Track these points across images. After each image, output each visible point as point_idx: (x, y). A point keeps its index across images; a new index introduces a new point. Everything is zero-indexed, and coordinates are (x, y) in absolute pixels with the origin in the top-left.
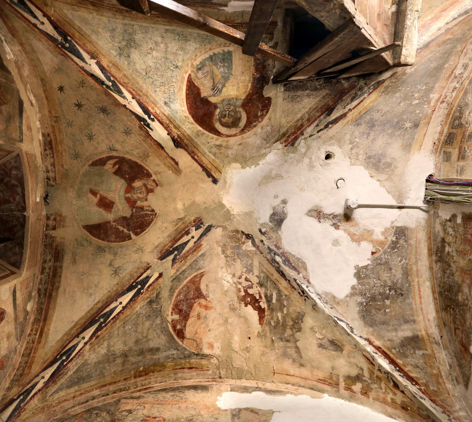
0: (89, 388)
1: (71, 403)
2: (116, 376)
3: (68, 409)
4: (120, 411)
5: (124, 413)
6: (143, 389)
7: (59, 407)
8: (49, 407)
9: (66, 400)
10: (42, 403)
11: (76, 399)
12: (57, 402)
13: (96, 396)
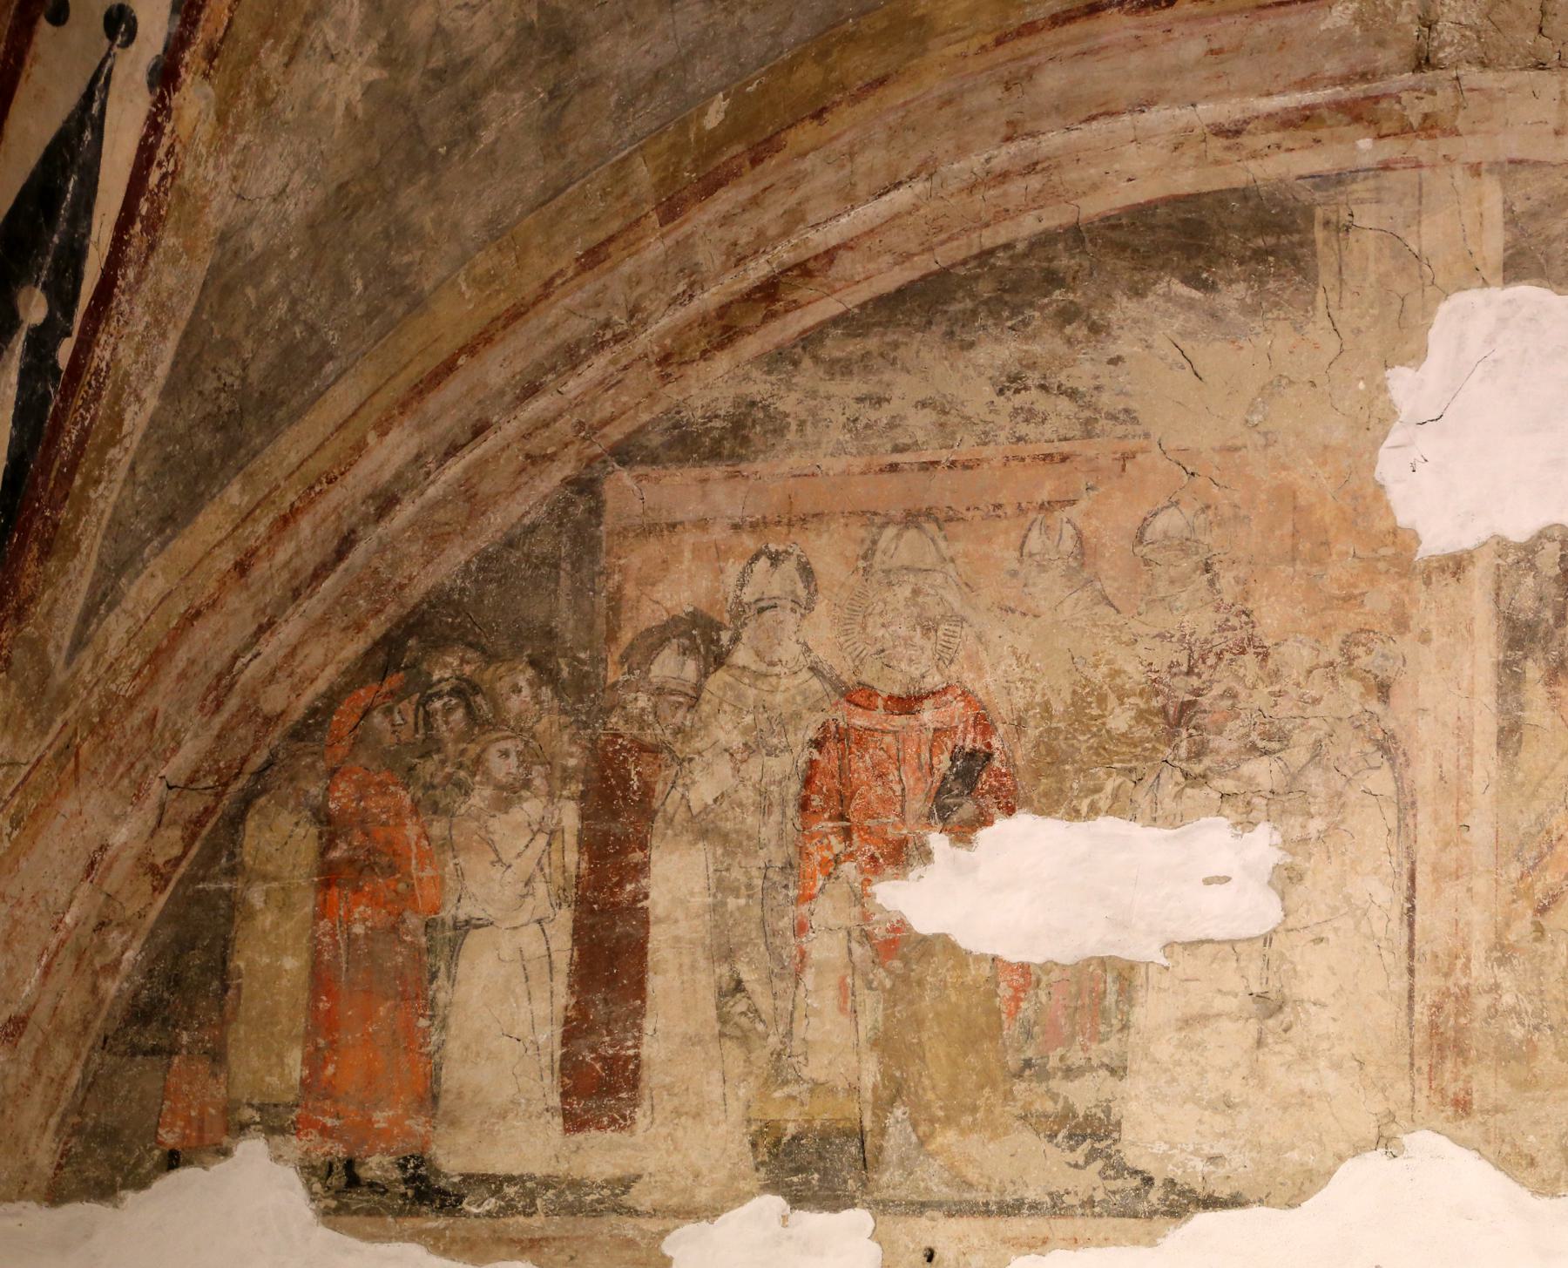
0: (328, 453)
1: (240, 610)
2: (510, 261)
3: (235, 658)
4: (626, 636)
5: (671, 666)
6: (748, 297)
7: (167, 682)
8: (99, 725)
9: (193, 616)
10: (43, 728)
11: (260, 570)
12: (136, 660)
13: (398, 476)
